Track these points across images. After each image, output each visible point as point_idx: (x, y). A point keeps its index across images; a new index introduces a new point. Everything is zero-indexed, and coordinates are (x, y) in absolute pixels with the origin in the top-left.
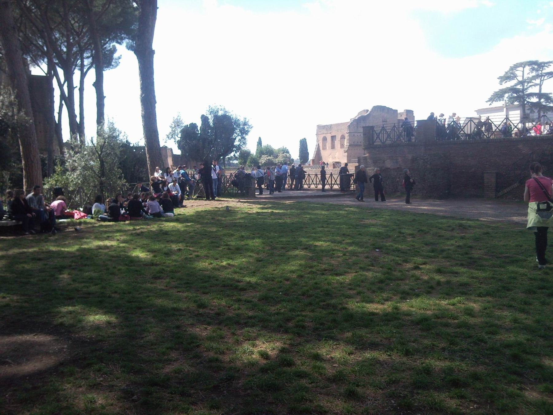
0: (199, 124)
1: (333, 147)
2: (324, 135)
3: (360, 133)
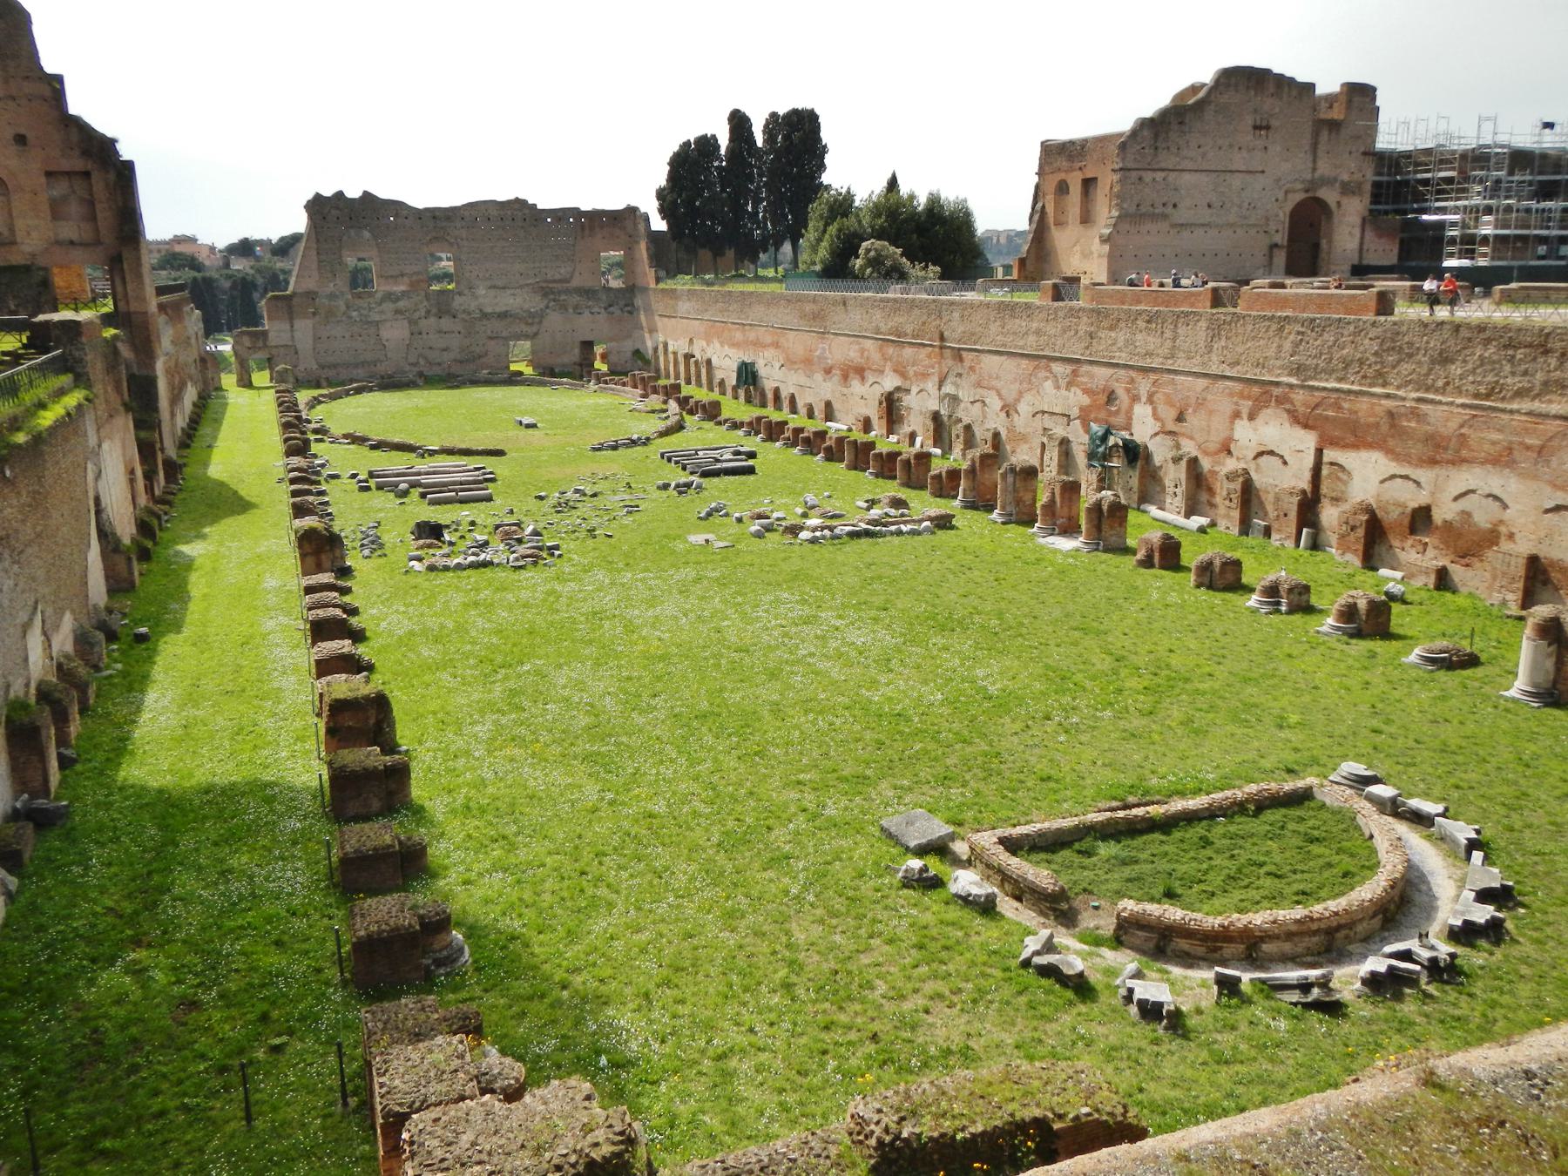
0: (724, 141)
1: (1086, 219)
2: (1062, 176)
3: (1163, 170)
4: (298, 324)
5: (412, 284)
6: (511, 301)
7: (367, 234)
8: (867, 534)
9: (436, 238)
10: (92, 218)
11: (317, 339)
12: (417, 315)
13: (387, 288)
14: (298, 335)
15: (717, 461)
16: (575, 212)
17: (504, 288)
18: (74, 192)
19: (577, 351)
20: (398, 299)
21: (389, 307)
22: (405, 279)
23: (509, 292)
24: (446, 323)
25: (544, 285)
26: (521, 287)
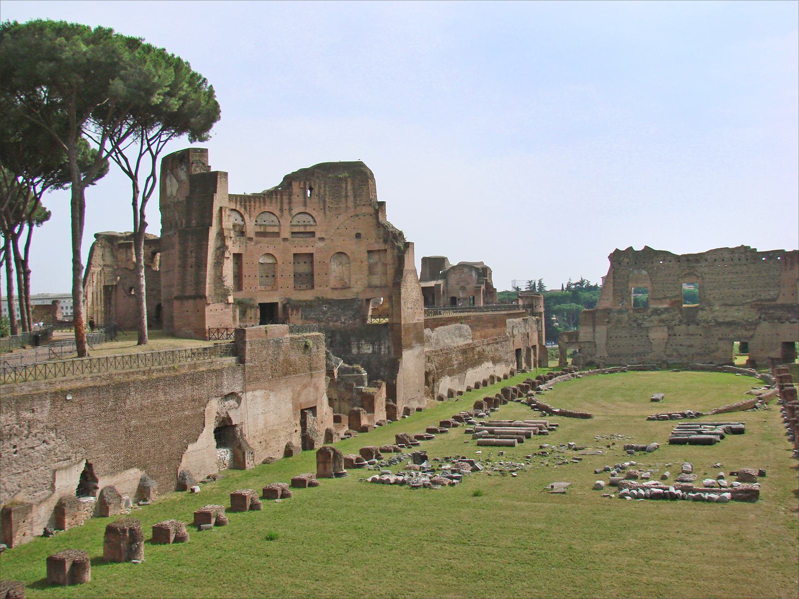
4: (598, 328)
5: (673, 304)
6: (735, 314)
7: (644, 272)
8: (674, 497)
9: (689, 274)
10: (385, 273)
11: (609, 337)
12: (673, 323)
13: (655, 306)
14: (597, 335)
15: (700, 433)
16: (781, 253)
17: (731, 305)
18: (380, 260)
19: (780, 349)
20: (662, 313)
21: (655, 318)
22: (667, 300)
23: (737, 307)
24: (692, 328)
25: (759, 303)
26: (743, 305)
